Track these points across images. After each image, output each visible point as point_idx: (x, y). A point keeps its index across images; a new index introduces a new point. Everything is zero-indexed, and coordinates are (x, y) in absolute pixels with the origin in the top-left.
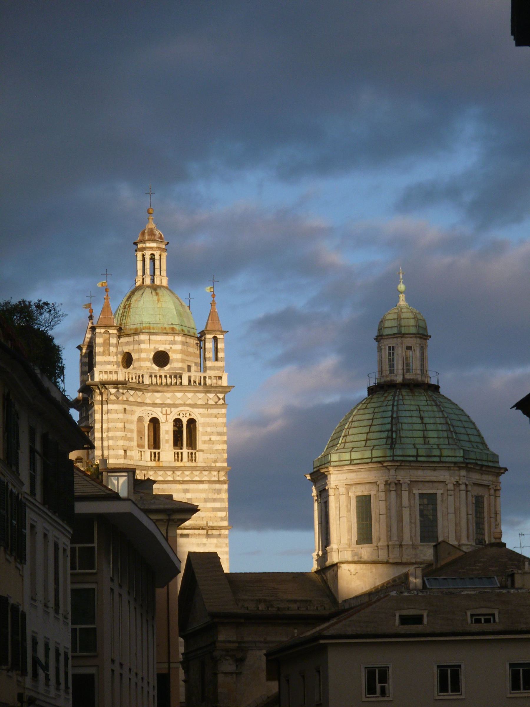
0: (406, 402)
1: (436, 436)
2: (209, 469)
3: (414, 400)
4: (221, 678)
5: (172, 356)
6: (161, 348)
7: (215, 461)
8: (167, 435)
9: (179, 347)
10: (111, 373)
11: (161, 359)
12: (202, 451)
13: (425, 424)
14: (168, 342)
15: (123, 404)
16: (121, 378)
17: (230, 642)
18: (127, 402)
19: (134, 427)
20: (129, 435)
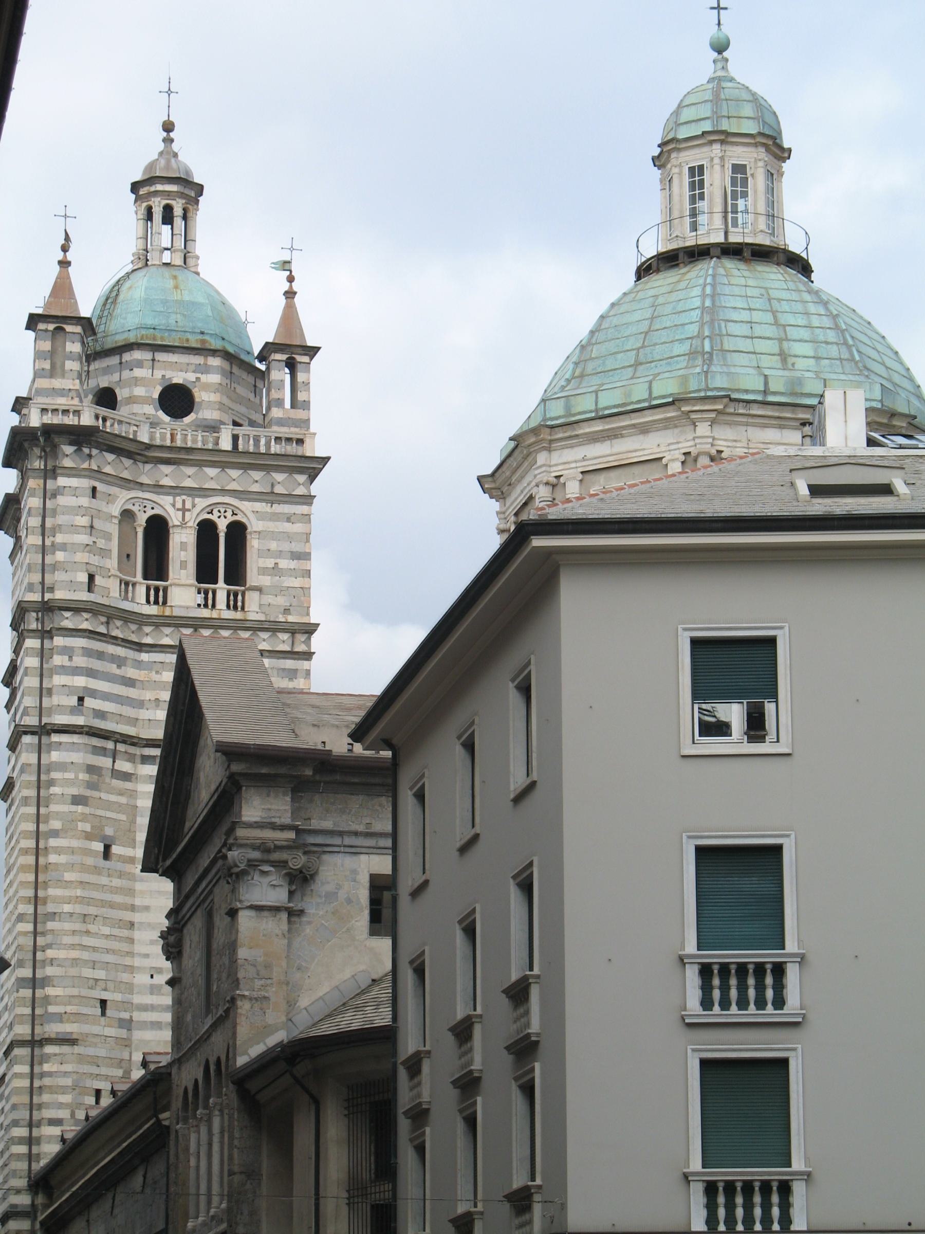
0: (734, 281)
1: (812, 354)
2: (273, 628)
3: (757, 278)
4: (245, 919)
5: (200, 395)
6: (178, 379)
7: (287, 611)
8: (183, 553)
9: (214, 378)
10: (66, 412)
11: (177, 400)
12: (259, 589)
13: (784, 326)
14: (192, 368)
15: (90, 477)
16: (87, 419)
17: (273, 827)
18: (98, 474)
19: (113, 529)
20: (101, 543)
